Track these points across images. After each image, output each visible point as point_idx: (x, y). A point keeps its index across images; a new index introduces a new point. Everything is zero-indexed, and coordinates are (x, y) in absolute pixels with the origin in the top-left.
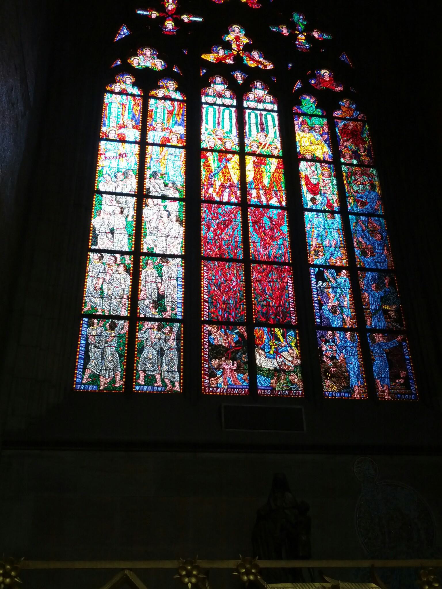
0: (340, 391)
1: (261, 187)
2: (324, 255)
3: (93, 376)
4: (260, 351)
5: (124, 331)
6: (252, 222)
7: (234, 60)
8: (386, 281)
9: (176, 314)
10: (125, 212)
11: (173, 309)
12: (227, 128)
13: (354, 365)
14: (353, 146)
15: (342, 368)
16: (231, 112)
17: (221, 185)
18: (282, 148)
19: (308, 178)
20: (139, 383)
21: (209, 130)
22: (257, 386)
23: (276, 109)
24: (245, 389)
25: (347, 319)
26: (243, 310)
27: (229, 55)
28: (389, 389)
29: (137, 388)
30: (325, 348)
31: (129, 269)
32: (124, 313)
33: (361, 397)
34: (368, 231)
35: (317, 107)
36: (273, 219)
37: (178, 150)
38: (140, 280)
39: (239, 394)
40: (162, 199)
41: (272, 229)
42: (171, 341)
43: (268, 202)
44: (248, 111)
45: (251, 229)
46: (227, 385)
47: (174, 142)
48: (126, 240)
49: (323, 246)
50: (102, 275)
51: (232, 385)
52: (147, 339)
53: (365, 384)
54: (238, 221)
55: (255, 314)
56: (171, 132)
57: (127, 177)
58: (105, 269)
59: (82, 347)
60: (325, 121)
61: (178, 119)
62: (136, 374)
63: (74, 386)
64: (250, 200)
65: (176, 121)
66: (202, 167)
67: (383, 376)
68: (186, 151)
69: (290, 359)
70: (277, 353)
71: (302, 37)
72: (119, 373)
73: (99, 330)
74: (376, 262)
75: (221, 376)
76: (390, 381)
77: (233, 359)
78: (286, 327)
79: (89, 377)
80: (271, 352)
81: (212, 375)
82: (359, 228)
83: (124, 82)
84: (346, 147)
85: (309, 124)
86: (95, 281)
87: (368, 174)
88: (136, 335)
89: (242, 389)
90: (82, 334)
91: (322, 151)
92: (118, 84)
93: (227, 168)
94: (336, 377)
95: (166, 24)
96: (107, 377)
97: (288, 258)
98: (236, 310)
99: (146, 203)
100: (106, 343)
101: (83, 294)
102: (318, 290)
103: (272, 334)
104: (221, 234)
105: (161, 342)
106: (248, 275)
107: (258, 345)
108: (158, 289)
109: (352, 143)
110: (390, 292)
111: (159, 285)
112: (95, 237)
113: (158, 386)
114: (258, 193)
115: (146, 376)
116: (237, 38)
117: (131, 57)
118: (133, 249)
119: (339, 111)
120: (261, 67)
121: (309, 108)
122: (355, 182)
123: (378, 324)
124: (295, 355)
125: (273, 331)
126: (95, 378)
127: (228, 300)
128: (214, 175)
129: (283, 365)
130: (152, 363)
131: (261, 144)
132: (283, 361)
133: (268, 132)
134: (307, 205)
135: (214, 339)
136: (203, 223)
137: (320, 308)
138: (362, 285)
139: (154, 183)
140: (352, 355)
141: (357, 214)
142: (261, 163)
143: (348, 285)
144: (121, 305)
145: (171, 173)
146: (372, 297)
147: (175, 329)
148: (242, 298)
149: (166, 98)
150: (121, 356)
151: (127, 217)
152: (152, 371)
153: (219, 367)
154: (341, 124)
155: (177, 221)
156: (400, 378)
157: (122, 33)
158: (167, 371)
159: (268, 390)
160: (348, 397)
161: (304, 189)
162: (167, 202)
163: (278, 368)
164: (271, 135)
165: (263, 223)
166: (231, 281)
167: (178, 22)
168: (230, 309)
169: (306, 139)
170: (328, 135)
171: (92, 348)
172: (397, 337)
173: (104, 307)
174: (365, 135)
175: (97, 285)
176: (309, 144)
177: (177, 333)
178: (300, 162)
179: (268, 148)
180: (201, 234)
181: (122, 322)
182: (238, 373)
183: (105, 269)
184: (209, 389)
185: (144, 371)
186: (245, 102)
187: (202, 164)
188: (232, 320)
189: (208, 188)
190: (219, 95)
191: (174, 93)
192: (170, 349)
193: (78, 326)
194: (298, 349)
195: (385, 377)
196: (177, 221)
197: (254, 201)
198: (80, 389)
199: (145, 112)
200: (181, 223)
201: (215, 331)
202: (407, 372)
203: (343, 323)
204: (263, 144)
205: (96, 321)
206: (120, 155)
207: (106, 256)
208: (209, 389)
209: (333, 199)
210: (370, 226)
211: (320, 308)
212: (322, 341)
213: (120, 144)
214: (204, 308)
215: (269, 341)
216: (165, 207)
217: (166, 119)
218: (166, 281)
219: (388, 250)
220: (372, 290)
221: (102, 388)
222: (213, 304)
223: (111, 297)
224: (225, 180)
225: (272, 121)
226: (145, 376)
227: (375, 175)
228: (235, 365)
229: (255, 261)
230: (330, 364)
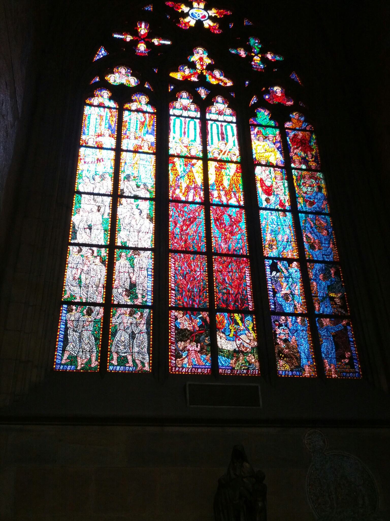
0: (292, 371)
1: (221, 189)
2: (277, 248)
3: (71, 357)
4: (221, 334)
5: (99, 317)
6: (214, 219)
7: (198, 78)
8: (332, 272)
9: (146, 301)
10: (102, 210)
11: (143, 297)
12: (192, 137)
13: (305, 347)
14: (302, 153)
16: (195, 123)
18: (241, 154)
19: (263, 181)
20: (112, 363)
22: (218, 366)
24: (208, 368)
25: (298, 306)
26: (206, 298)
27: (195, 74)
29: (111, 368)
30: (279, 331)
31: (105, 261)
32: (100, 300)
33: (310, 376)
34: (316, 228)
35: (270, 119)
36: (232, 217)
37: (148, 156)
38: (114, 270)
39: (202, 373)
40: (135, 199)
41: (231, 226)
42: (142, 325)
43: (227, 202)
44: (210, 122)
45: (213, 225)
46: (192, 365)
47: (146, 150)
48: (102, 235)
50: (80, 266)
51: (196, 365)
52: (120, 323)
53: (315, 364)
55: (217, 301)
56: (143, 140)
57: (103, 179)
58: (83, 260)
59: (62, 331)
60: (278, 131)
61: (149, 129)
62: (110, 355)
63: (54, 366)
65: (148, 131)
66: (170, 171)
67: (330, 356)
71: (257, 59)
72: (94, 354)
73: (77, 316)
74: (323, 255)
75: (186, 357)
76: (337, 361)
77: (197, 342)
78: (244, 312)
81: (178, 356)
83: (102, 96)
84: (296, 154)
85: (264, 134)
86: (74, 271)
87: (316, 178)
88: (110, 320)
89: (205, 368)
90: (61, 319)
91: (276, 157)
92: (96, 98)
94: (288, 358)
95: (139, 46)
96: (84, 358)
97: (245, 251)
98: (200, 297)
99: (120, 202)
100: (83, 327)
101: (63, 283)
102: (272, 280)
103: (232, 319)
104: (187, 230)
105: (133, 326)
107: (219, 329)
108: (130, 278)
109: (301, 150)
110: (336, 281)
111: (131, 275)
112: (75, 232)
113: (129, 367)
114: (219, 194)
116: (201, 59)
117: (108, 75)
118: (108, 243)
119: (290, 122)
120: (222, 84)
121: (264, 119)
122: (304, 184)
124: (252, 338)
126: (73, 360)
127: (193, 288)
128: (180, 178)
130: (125, 345)
131: (222, 151)
132: (241, 343)
133: (227, 141)
134: (262, 204)
135: (180, 323)
136: (170, 220)
137: (274, 296)
138: (311, 276)
139: (128, 185)
141: (306, 213)
142: (222, 168)
143: (299, 275)
144: (97, 293)
145: (143, 175)
146: (320, 285)
147: (145, 315)
148: (205, 286)
149: (138, 111)
150: (96, 339)
151: (103, 214)
152: (125, 353)
153: (184, 349)
154: (291, 134)
155: (147, 218)
156: (345, 358)
157: (100, 54)
158: (138, 353)
159: (228, 369)
160: (300, 375)
161: (260, 190)
162: (139, 202)
163: (237, 349)
164: (230, 144)
165: (223, 220)
166: (195, 271)
167: (150, 45)
168: (194, 297)
169: (261, 147)
170: (280, 143)
171: (70, 332)
172: (342, 322)
173: (82, 295)
174: (312, 143)
175: (75, 275)
177: (147, 318)
178: (256, 167)
179: (227, 155)
180: (169, 229)
181: (97, 308)
182: (201, 354)
183: (83, 260)
184: (175, 369)
185: (117, 353)
186: (207, 114)
187: (170, 168)
188: (196, 306)
189: (175, 190)
190: (185, 108)
192: (140, 332)
193: (59, 311)
194: (254, 332)
196: (147, 218)
197: (215, 200)
198: (59, 369)
200: (151, 220)
201: (181, 316)
202: (352, 353)
203: (294, 309)
205: (74, 307)
206: (98, 160)
207: (84, 249)
208: (175, 369)
209: (285, 200)
210: (317, 223)
211: (274, 296)
212: (276, 325)
213: (98, 150)
214: (171, 295)
216: (138, 205)
217: (138, 129)
218: (137, 271)
219: (333, 244)
220: (320, 280)
221: (79, 368)
222: (180, 291)
223: (88, 286)
224: (190, 182)
225: (232, 131)
226: (118, 357)
228: (199, 347)
229: (217, 254)
230: (283, 345)
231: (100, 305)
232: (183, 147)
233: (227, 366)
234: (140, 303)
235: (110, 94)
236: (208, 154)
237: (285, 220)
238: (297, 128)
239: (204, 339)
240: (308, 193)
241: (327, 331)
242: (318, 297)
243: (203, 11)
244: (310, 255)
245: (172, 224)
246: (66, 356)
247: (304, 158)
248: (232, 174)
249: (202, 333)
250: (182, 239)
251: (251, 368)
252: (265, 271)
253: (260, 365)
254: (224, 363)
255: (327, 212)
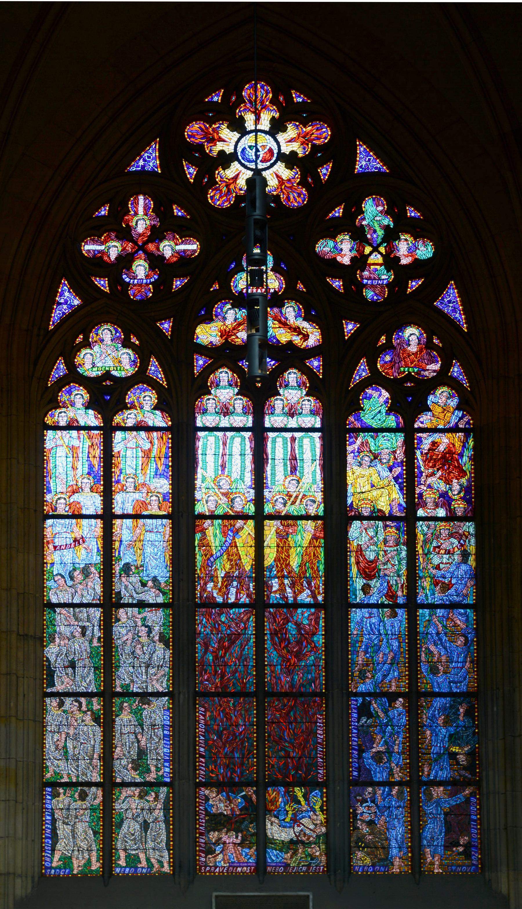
0: (373, 866)
2: (373, 676)
3: (64, 858)
4: (273, 819)
5: (98, 801)
9: (162, 776)
11: (158, 769)
13: (398, 832)
15: (382, 834)
17: (225, 574)
18: (325, 500)
19: (361, 550)
20: (119, 864)
21: (209, 479)
23: (318, 425)
25: (396, 770)
28: (441, 860)
32: (96, 778)
33: (401, 872)
34: (446, 634)
35: (388, 413)
37: (159, 521)
39: (243, 873)
41: (299, 643)
42: (157, 811)
43: (295, 598)
44: (271, 435)
45: (268, 645)
46: (229, 863)
47: (155, 511)
48: (92, 676)
49: (373, 664)
54: (250, 632)
58: (67, 719)
59: (48, 824)
60: (400, 438)
62: (116, 854)
64: (269, 598)
65: (157, 469)
66: (197, 549)
67: (435, 843)
68: (172, 523)
69: (312, 827)
70: (295, 820)
73: (66, 802)
74: (450, 682)
75: (221, 852)
76: (445, 850)
78: (310, 785)
79: (60, 860)
80: (288, 820)
81: (209, 851)
82: (432, 630)
85: (372, 449)
86: (56, 736)
87: (460, 535)
91: (389, 498)
92: (64, 410)
93: (236, 546)
94: (371, 848)
95: (134, 268)
100: (76, 817)
103: (290, 796)
105: (145, 813)
106: (261, 715)
108: (138, 742)
110: (464, 726)
111: (139, 737)
112: (51, 674)
113: (143, 868)
114: (282, 584)
115: (128, 856)
120: (297, 340)
122: (437, 550)
123: (440, 773)
124: (319, 822)
125: (291, 791)
126: (67, 860)
127: (232, 752)
128: (215, 560)
129: (302, 836)
132: (302, 830)
134: (356, 598)
135: (212, 806)
136: (198, 640)
137: (360, 757)
139: (127, 583)
140: (396, 818)
141: (432, 607)
143: (404, 720)
146: (437, 735)
147: (162, 796)
148: (252, 749)
150: (95, 833)
151: (91, 641)
152: (135, 850)
153: (218, 841)
154: (426, 446)
155: (160, 641)
156: (458, 845)
158: (154, 849)
160: (385, 872)
161: (354, 570)
163: (295, 839)
164: (307, 479)
165: (286, 634)
166: (237, 725)
167: (156, 261)
169: (365, 479)
171: (59, 824)
172: (464, 791)
173: (70, 772)
174: (465, 459)
175: (58, 742)
176: (368, 487)
177: (165, 800)
181: (94, 789)
182: (243, 847)
183: (67, 719)
184: (205, 869)
185: (125, 850)
186: (267, 418)
187: (196, 542)
188: (237, 780)
189: (206, 584)
190: (226, 411)
191: (152, 416)
192: (156, 820)
193: (42, 797)
194: (323, 814)
195: (437, 846)
196: (160, 641)
197: (275, 597)
199: (108, 457)
200: (167, 645)
201: (214, 795)
202: (471, 838)
203: (390, 775)
204: (294, 495)
205: (61, 791)
207: (68, 701)
208: (205, 869)
210: (450, 624)
211: (360, 757)
212: (358, 801)
213: (74, 521)
214: (200, 765)
215: (285, 805)
216: (144, 619)
219: (471, 662)
223: (78, 759)
225: (311, 447)
226: (126, 856)
227: (472, 535)
228: (239, 838)
229: (273, 694)
231: (97, 785)
232: (220, 495)
233: (280, 863)
234: (155, 779)
235: (87, 396)
236: (266, 505)
237: (393, 626)
238: (441, 427)
239: (247, 827)
240: (442, 566)
241: (436, 806)
242: (430, 754)
243: (268, 137)
244: (427, 683)
245: (200, 648)
246: (57, 856)
247: (444, 495)
248: (305, 543)
249: (244, 818)
250: (216, 672)
251: (314, 863)
252: (349, 715)
253: (327, 860)
254: (274, 858)
255: (471, 602)
